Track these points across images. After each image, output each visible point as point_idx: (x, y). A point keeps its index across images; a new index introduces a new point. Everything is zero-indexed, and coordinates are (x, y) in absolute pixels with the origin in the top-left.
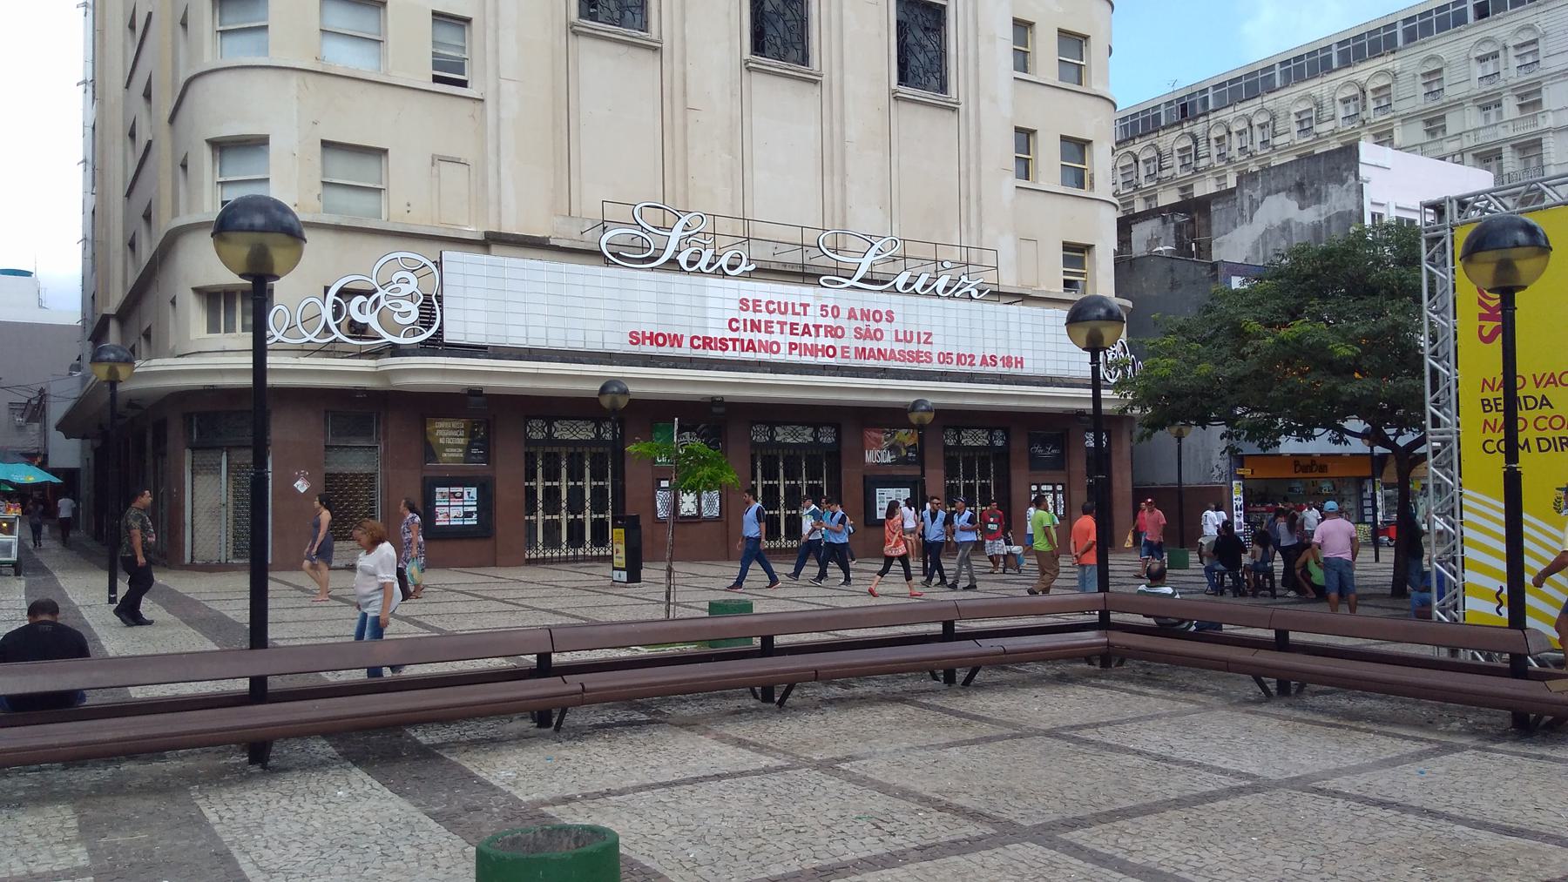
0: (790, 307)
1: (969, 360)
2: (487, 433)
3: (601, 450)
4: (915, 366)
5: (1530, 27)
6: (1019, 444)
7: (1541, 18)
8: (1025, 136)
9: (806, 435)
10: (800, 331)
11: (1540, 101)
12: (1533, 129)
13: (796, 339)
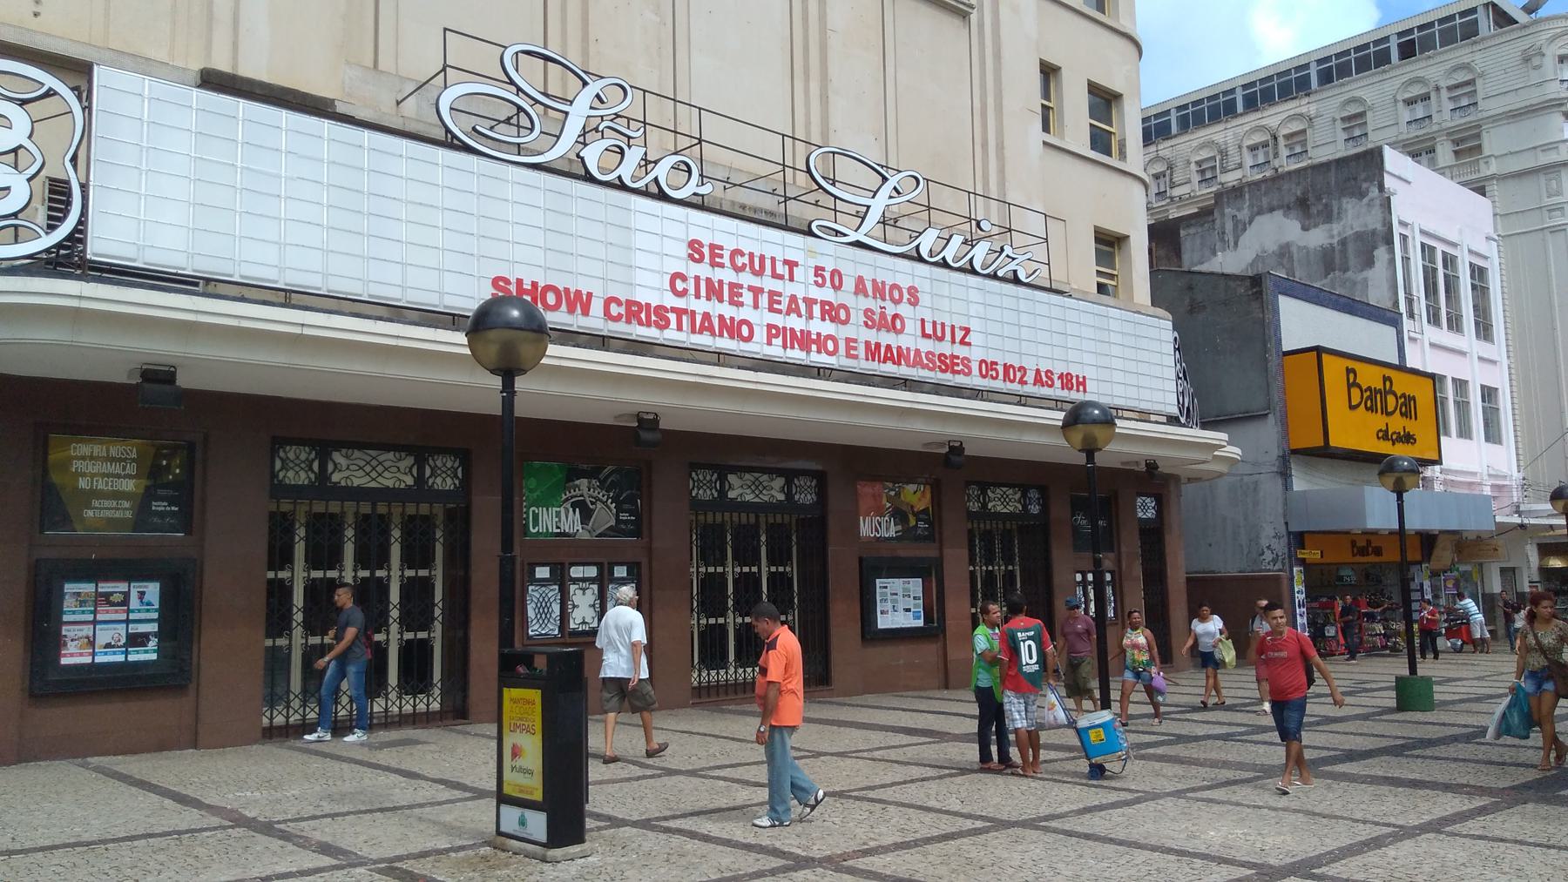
0: (768, 263)
1: (1019, 375)
2: (189, 467)
3: (424, 509)
4: (948, 378)
5: (1466, 67)
6: (1060, 510)
7: (1478, 56)
8: (1049, 72)
10: (783, 307)
11: (1480, 146)
12: (1474, 177)
13: (778, 320)
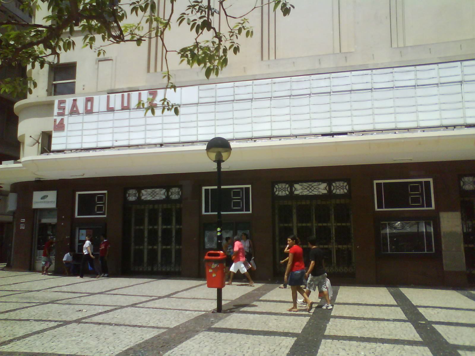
3: (169, 206)
9: (321, 189)
